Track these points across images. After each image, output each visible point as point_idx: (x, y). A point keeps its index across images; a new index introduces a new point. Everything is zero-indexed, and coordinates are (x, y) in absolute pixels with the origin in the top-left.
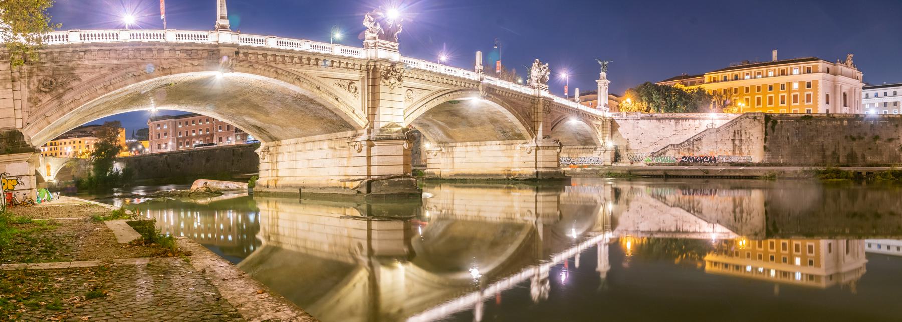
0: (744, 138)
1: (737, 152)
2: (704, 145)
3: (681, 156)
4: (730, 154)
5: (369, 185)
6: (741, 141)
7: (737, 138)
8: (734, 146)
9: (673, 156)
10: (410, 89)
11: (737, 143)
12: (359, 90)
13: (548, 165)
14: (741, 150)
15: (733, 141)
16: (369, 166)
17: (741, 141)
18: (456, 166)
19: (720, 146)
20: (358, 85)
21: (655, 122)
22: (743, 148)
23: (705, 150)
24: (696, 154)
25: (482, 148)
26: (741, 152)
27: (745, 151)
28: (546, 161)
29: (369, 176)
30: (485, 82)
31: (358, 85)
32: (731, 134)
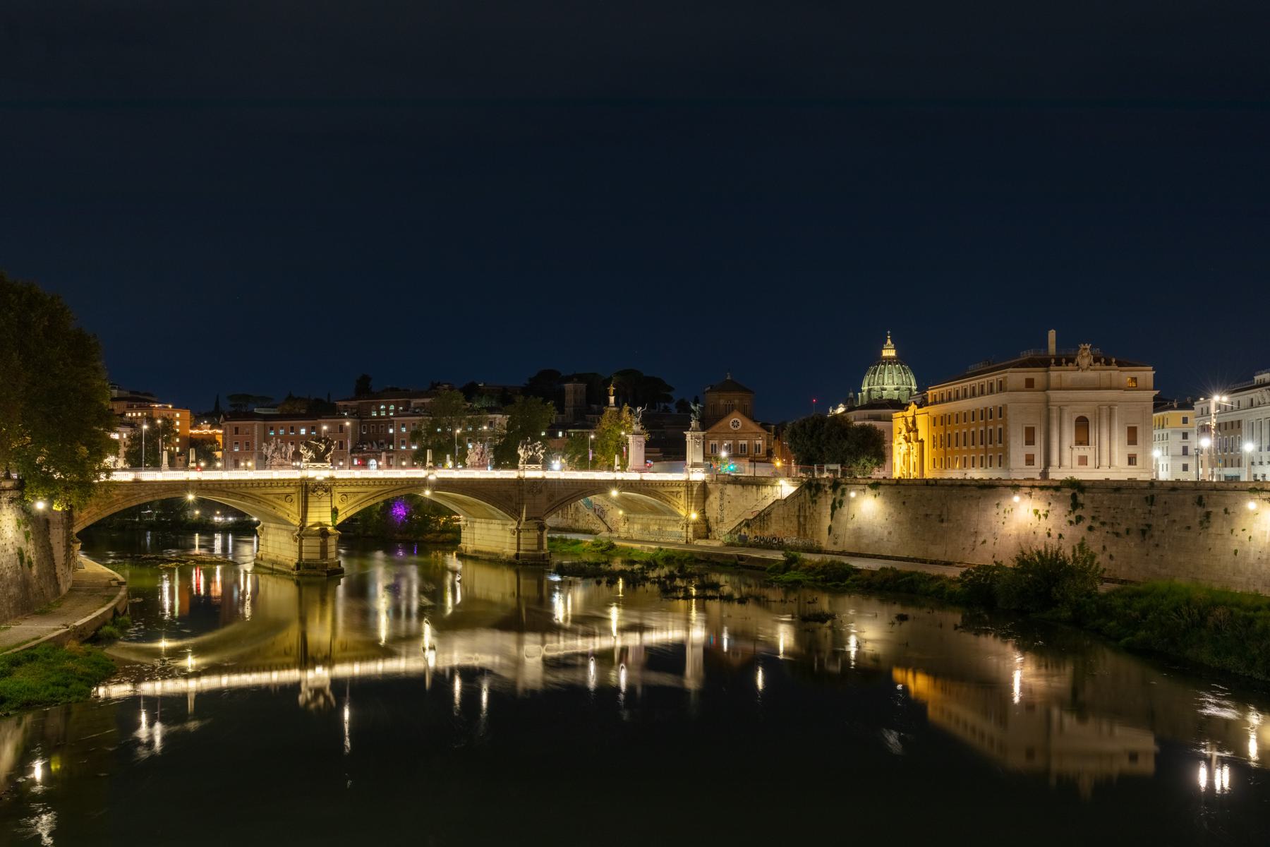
5: (298, 566)
6: (805, 517)
10: (345, 494)
12: (295, 500)
13: (529, 547)
15: (799, 517)
16: (301, 552)
17: (805, 517)
18: (477, 542)
19: (787, 524)
20: (295, 497)
21: (739, 487)
23: (774, 529)
24: (766, 534)
25: (491, 526)
26: (805, 535)
28: (529, 541)
29: (300, 559)
30: (432, 478)
31: (295, 497)
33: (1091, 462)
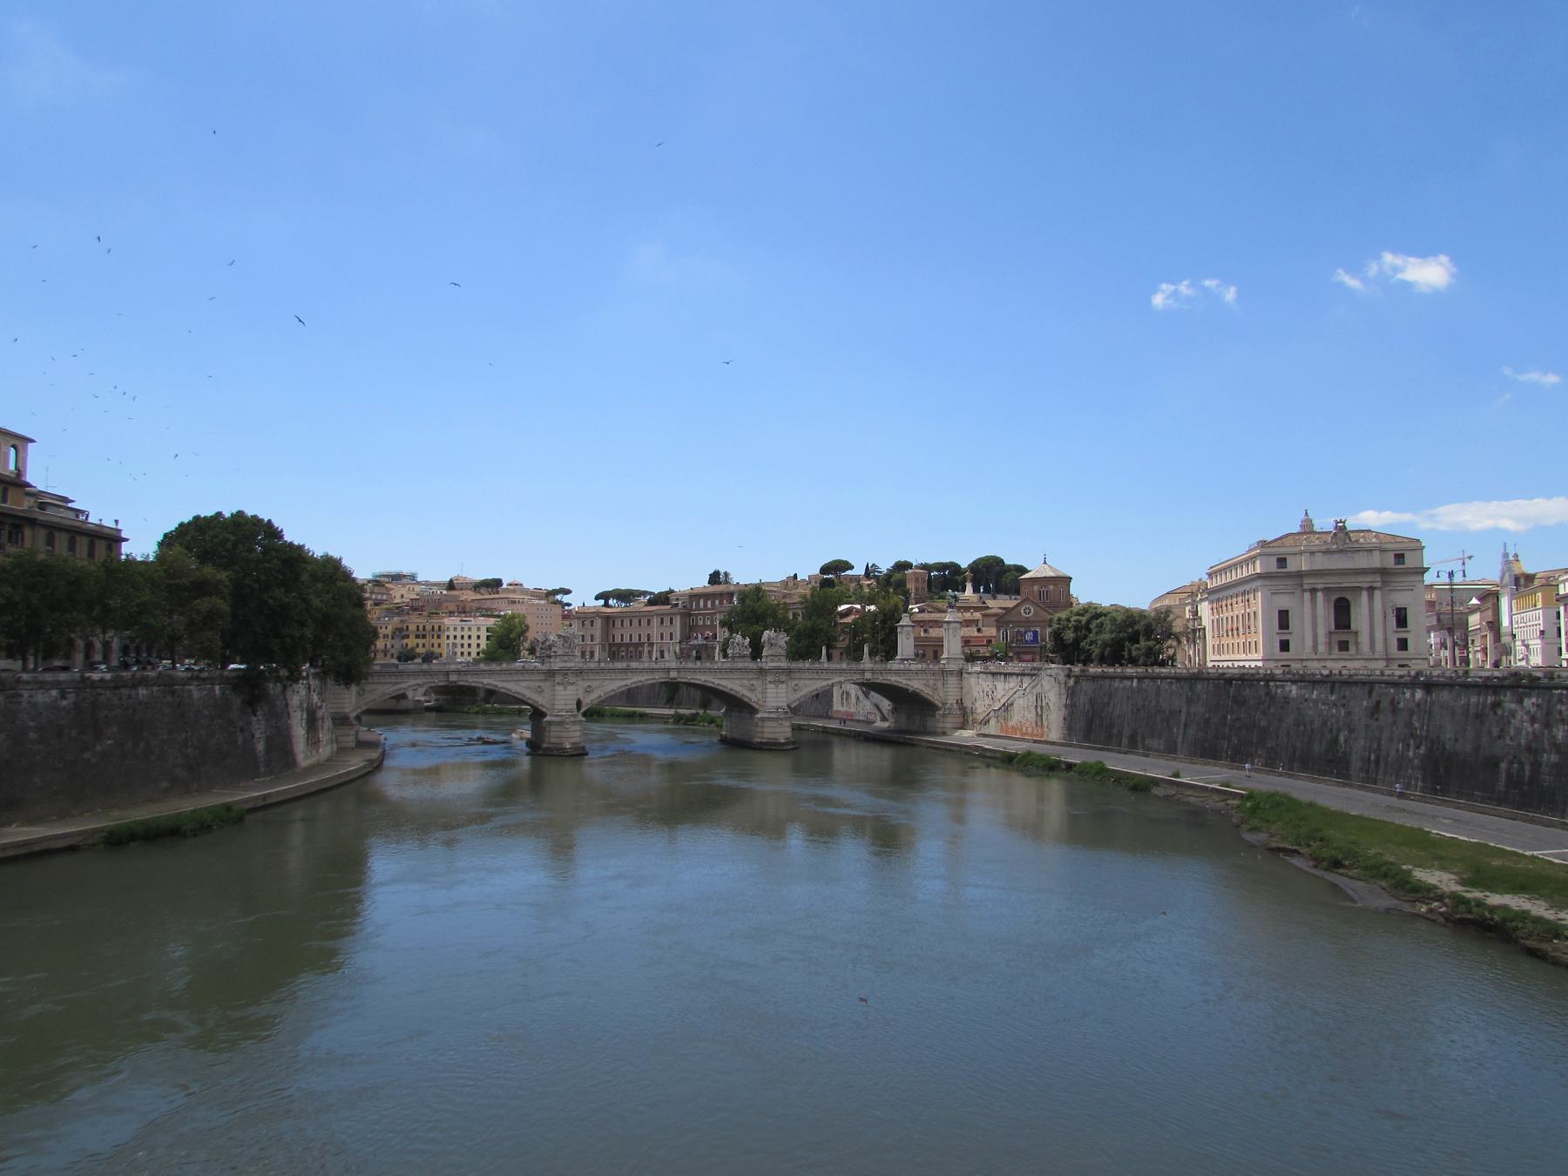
33: (1352, 647)
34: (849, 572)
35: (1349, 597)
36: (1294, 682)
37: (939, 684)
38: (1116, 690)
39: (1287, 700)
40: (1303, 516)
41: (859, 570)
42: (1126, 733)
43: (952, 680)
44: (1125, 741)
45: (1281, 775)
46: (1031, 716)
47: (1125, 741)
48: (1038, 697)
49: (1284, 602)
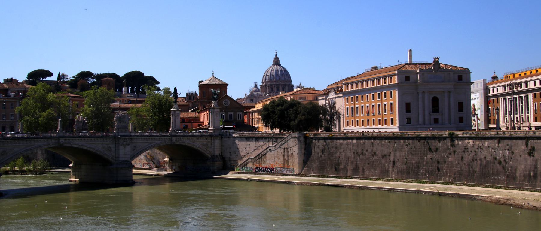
0: (289, 153)
1: (286, 164)
2: (267, 158)
3: (255, 167)
4: (282, 166)
6: (288, 155)
7: (286, 153)
8: (284, 159)
9: (251, 166)
11: (286, 157)
14: (288, 162)
15: (284, 155)
19: (276, 160)
22: (290, 161)
24: (263, 166)
26: (288, 166)
27: (291, 164)
32: (283, 150)
34: (48, 79)
35: (438, 97)
36: (470, 138)
37: (209, 144)
38: (341, 145)
39: (466, 149)
40: (274, 56)
41: (54, 78)
42: (350, 167)
43: (217, 142)
44: (349, 173)
45: (467, 185)
46: (280, 161)
47: (349, 173)
48: (285, 149)
49: (408, 99)
